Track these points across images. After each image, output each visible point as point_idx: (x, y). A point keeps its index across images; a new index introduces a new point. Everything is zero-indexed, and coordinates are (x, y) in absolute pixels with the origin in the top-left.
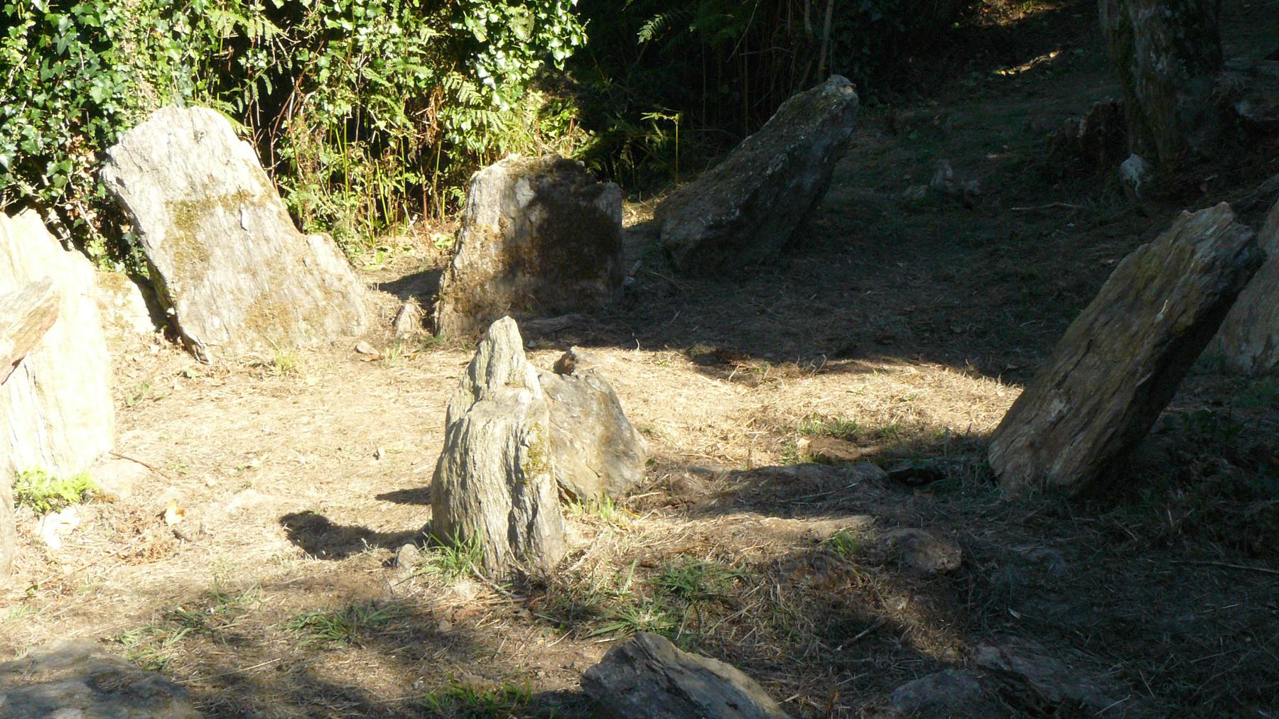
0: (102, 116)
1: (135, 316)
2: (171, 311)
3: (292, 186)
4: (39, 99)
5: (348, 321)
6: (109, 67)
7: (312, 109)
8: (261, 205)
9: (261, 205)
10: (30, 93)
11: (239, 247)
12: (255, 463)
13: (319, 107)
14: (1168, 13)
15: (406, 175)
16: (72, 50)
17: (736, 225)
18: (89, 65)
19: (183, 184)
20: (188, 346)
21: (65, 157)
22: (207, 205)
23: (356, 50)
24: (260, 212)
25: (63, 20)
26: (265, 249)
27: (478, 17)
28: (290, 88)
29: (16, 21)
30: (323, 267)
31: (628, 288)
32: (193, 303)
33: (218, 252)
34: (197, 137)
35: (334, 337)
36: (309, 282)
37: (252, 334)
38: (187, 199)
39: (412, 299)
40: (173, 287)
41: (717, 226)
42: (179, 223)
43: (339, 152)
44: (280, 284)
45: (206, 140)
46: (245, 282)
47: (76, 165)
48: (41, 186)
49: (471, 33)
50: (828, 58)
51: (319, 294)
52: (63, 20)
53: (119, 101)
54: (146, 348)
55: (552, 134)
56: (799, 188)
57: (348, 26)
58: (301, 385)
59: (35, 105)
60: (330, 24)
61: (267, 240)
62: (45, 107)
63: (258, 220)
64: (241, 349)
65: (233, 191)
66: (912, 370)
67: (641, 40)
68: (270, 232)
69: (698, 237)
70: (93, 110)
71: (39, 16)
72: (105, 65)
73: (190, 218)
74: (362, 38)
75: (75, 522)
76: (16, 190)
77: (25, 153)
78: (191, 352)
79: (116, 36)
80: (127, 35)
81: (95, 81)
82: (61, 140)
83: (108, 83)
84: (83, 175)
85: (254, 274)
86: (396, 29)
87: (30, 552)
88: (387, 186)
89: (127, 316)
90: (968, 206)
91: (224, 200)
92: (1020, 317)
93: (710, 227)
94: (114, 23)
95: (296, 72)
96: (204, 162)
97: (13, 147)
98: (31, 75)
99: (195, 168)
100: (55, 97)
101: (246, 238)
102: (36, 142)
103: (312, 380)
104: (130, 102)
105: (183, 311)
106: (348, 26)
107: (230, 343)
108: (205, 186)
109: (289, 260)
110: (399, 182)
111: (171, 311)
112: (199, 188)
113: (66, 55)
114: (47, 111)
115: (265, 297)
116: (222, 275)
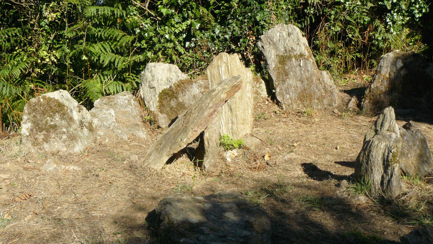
0: (259, 25)
1: (262, 91)
2: (274, 91)
3: (317, 54)
4: (240, 18)
5: (331, 101)
6: (263, 10)
7: (327, 28)
8: (307, 59)
9: (307, 59)
10: (237, 16)
11: (298, 72)
12: (295, 144)
13: (329, 28)
15: (357, 54)
16: (252, 3)
18: (257, 8)
19: (283, 50)
20: (278, 103)
21: (246, 38)
22: (290, 58)
23: (344, 9)
24: (307, 61)
26: (307, 74)
28: (321, 21)
30: (326, 82)
32: (281, 89)
33: (292, 73)
34: (289, 34)
35: (326, 106)
36: (320, 87)
37: (299, 102)
38: (283, 55)
39: (354, 97)
40: (276, 83)
42: (280, 63)
43: (334, 44)
44: (311, 86)
45: (292, 36)
46: (299, 84)
47: (249, 40)
48: (238, 46)
51: (323, 91)
53: (265, 21)
55: (411, 44)
58: (313, 121)
59: (239, 20)
61: (308, 71)
62: (242, 21)
63: (306, 64)
65: (299, 54)
68: (309, 68)
70: (256, 23)
72: (262, 9)
73: (284, 61)
75: (236, 154)
76: (230, 47)
77: (234, 35)
78: (278, 105)
81: (258, 14)
82: (245, 32)
83: (262, 15)
84: (251, 44)
85: (302, 82)
87: (222, 161)
88: (349, 57)
89: (259, 91)
91: (295, 56)
96: (290, 43)
97: (230, 33)
99: (287, 45)
100: (245, 18)
101: (301, 70)
104: (268, 21)
107: (292, 104)
108: (290, 51)
109: (314, 79)
110: (354, 56)
111: (274, 91)
112: (288, 51)
113: (250, 5)
114: (242, 22)
115: (305, 90)
116: (291, 81)
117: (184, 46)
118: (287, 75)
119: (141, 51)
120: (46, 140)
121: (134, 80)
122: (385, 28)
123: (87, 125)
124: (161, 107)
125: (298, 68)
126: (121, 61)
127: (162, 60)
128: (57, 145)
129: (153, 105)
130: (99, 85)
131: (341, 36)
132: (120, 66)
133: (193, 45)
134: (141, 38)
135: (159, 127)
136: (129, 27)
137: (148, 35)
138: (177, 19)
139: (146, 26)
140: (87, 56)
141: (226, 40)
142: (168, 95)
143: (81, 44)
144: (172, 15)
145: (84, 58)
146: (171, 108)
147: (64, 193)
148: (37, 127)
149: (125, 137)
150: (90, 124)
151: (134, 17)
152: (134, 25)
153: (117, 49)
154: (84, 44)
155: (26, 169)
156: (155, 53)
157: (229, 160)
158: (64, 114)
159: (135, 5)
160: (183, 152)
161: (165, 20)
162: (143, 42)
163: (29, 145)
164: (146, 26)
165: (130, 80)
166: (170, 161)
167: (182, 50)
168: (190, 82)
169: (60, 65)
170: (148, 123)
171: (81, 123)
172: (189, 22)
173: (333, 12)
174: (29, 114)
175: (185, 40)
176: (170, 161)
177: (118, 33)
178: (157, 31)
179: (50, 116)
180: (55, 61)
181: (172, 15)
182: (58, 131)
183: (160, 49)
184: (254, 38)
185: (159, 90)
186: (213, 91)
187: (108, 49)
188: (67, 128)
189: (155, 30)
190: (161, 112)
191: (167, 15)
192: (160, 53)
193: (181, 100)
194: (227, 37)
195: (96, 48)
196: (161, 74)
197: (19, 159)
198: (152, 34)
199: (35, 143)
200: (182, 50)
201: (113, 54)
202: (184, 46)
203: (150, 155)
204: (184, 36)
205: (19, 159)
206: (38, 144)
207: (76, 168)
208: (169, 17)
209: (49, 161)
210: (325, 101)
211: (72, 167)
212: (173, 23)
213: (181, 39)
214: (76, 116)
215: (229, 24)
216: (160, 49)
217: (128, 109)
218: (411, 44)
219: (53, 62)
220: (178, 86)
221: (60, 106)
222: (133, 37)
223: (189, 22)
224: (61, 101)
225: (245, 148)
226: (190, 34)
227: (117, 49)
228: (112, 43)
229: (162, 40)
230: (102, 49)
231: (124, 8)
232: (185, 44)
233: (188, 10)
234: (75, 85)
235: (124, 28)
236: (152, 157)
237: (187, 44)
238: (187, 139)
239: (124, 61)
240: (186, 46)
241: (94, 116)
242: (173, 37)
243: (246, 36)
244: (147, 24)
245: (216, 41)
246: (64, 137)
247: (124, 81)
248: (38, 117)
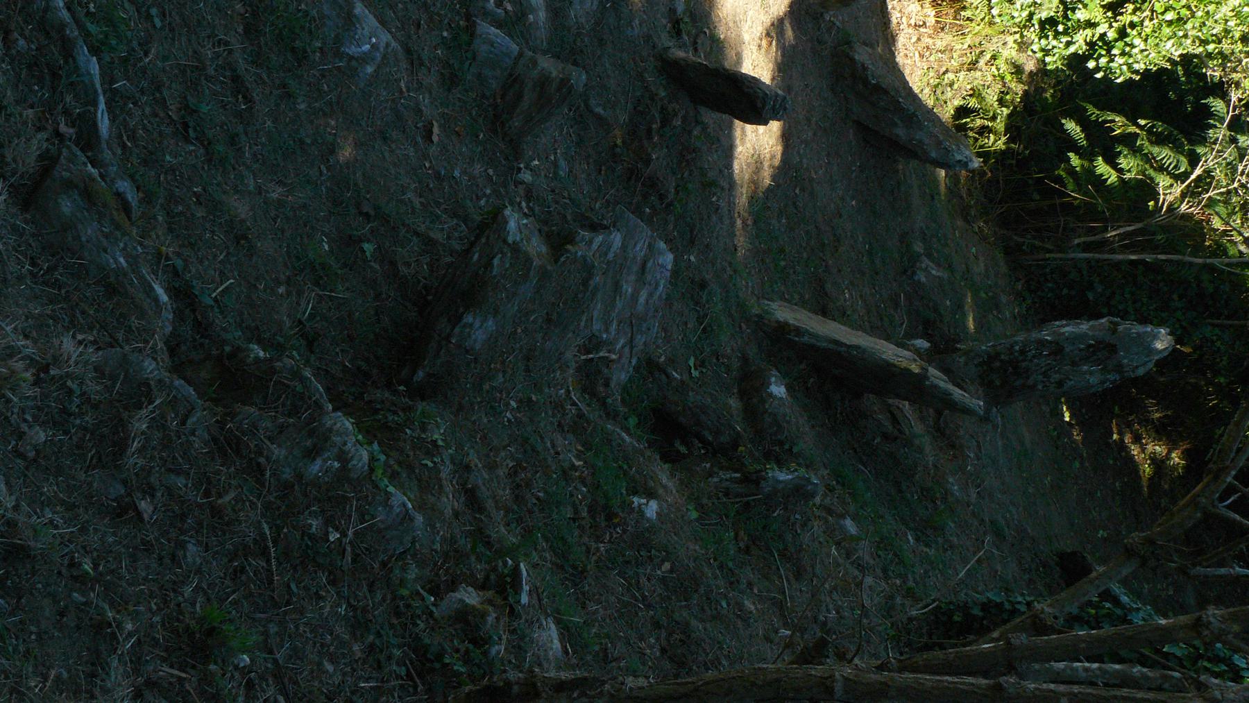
14: (1017, 348)
17: (866, 82)
31: (822, 14)
41: (864, 68)
50: (1055, 259)
56: (896, 125)
67: (1063, 121)
69: (857, 57)
90: (906, 271)
92: (807, 232)
93: (863, 65)
218: (994, 68)
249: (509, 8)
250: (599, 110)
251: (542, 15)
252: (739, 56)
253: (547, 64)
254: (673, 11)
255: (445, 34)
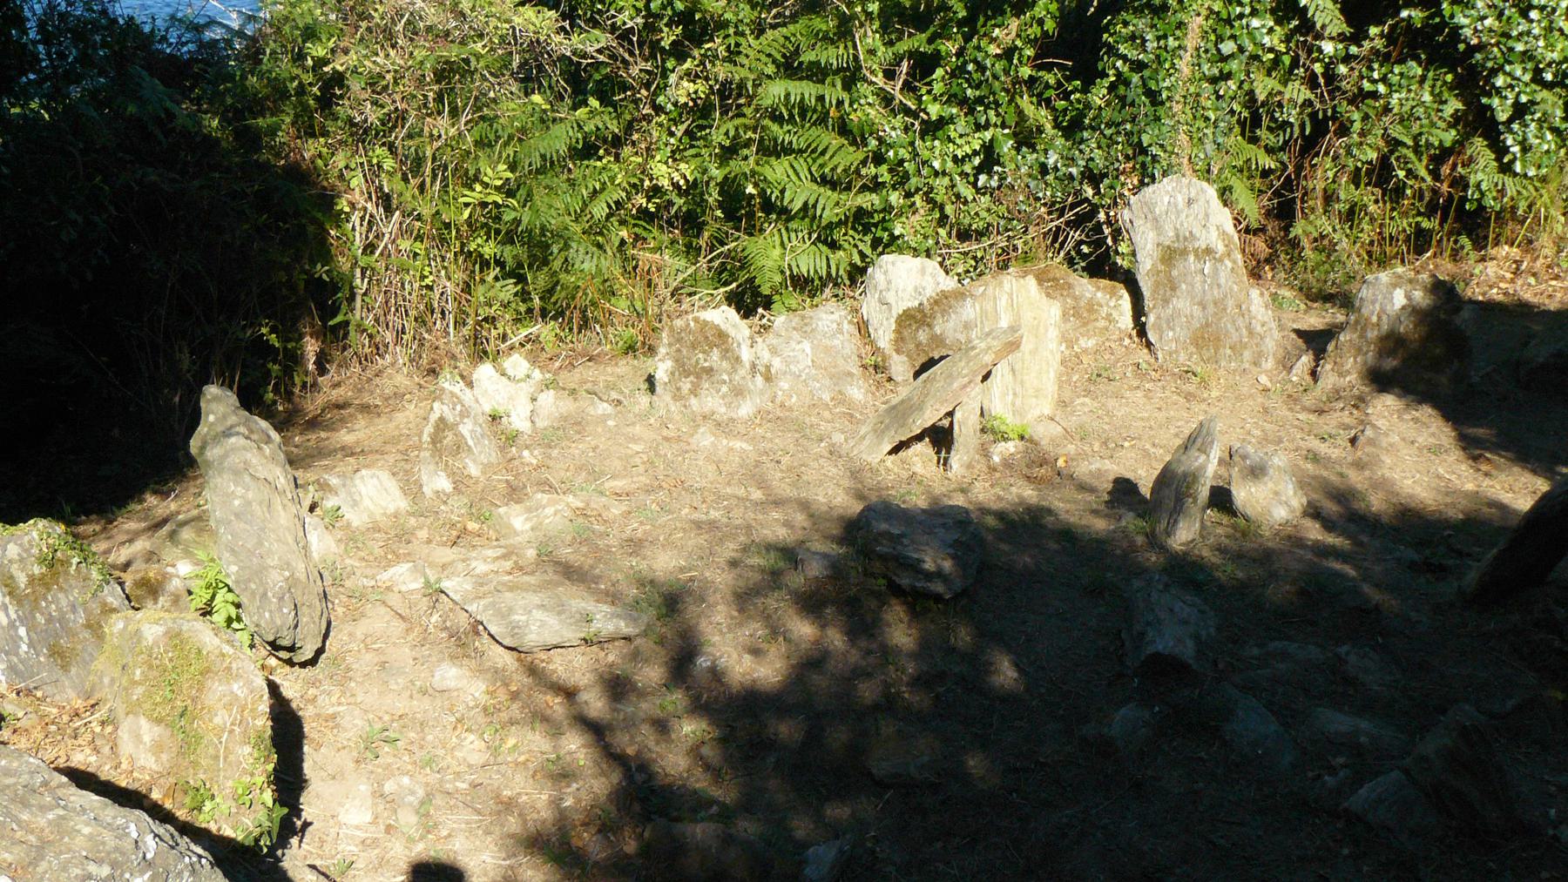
1: (1121, 314)
4: (1108, 132)
8: (1221, 260)
9: (1221, 260)
12: (1126, 444)
13: (1349, 153)
19: (1171, 234)
20: (1149, 345)
22: (1184, 253)
23: (1387, 110)
25: (1136, 79)
27: (1506, 98)
29: (1104, 75)
32: (1159, 318)
34: (1190, 202)
36: (1240, 322)
37: (1192, 349)
40: (1148, 303)
45: (1195, 206)
47: (1123, 185)
49: (1493, 110)
52: (1136, 79)
53: (1162, 146)
54: (1121, 339)
57: (1382, 88)
60: (1367, 86)
61: (1219, 286)
63: (1216, 271)
64: (1182, 357)
66: (1486, 510)
68: (1222, 281)
69: (1541, 360)
71: (1119, 74)
72: (1157, 119)
73: (1170, 258)
74: (1394, 101)
75: (1012, 450)
76: (1077, 193)
79: (1169, 98)
80: (1177, 98)
85: (1204, 308)
86: (1427, 98)
91: (1196, 251)
94: (1168, 88)
95: (1334, 118)
96: (1189, 223)
98: (1107, 114)
102: (1100, 162)
103: (1215, 393)
105: (1151, 320)
106: (1382, 88)
108: (1185, 239)
109: (1230, 303)
113: (1132, 104)
114: (1112, 142)
115: (1207, 325)
116: (1181, 303)
117: (975, 185)
118: (1173, 289)
119: (875, 186)
120: (694, 392)
121: (856, 246)
122: (1499, 159)
123: (763, 369)
124: (899, 340)
125: (1199, 278)
126: (830, 204)
127: (922, 212)
128: (711, 401)
129: (884, 337)
130: (778, 251)
131: (1380, 173)
132: (829, 216)
133: (994, 183)
134: (879, 159)
135: (890, 379)
136: (855, 130)
137: (896, 154)
138: (962, 125)
139: (893, 134)
140: (756, 185)
141: (1071, 177)
142: (913, 319)
143: (746, 158)
144: (951, 120)
145: (750, 189)
146: (918, 345)
147: (729, 484)
148: (682, 369)
149: (826, 397)
150: (768, 368)
151: (868, 111)
152: (866, 128)
153: (823, 177)
154: (752, 160)
155: (666, 439)
156: (908, 195)
157: (996, 459)
158: (727, 351)
159: (872, 83)
160: (919, 438)
161: (933, 128)
162: (884, 167)
163: (668, 398)
164: (893, 134)
165: (846, 245)
166: (895, 450)
167: (967, 192)
168: (960, 295)
169: (692, 190)
170: (871, 370)
171: (754, 366)
172: (988, 135)
173: (1356, 116)
174: (670, 345)
175: (979, 170)
176: (895, 450)
177: (833, 140)
178: (914, 149)
179: (704, 352)
180: (682, 182)
181: (951, 120)
182: (714, 379)
183: (918, 190)
184: (1136, 182)
185: (898, 309)
186: (973, 348)
187: (804, 173)
188: (730, 374)
189: (912, 144)
190: (898, 351)
191: (941, 118)
192: (917, 199)
193: (938, 330)
194: (1074, 171)
195: (777, 170)
196: (903, 279)
197: (652, 421)
198: (904, 153)
199: (678, 396)
200: (967, 192)
201: (815, 187)
202: (975, 185)
203: (864, 438)
204: (977, 161)
205: (652, 421)
206: (682, 398)
207: (744, 445)
208: (942, 123)
209: (702, 430)
210: (1247, 354)
211: (738, 444)
212: (953, 135)
213: (968, 168)
214: (746, 354)
215: (1082, 141)
216: (918, 190)
217: (836, 342)
219: (676, 186)
220: (936, 302)
221: (722, 335)
222: (860, 156)
223: (988, 135)
224: (723, 327)
225: (1031, 441)
226: (990, 157)
227: (823, 177)
228: (814, 161)
229: (925, 172)
230: (791, 172)
231: (847, 87)
232: (977, 180)
233: (987, 107)
234: (722, 244)
235: (843, 129)
236: (866, 442)
237: (983, 178)
238: (930, 416)
239: (837, 204)
240: (980, 184)
241: (774, 351)
242: (950, 164)
243: (1119, 173)
244: (894, 128)
245: (1050, 178)
246: (724, 389)
247: (834, 246)
248: (685, 352)
249: (1341, 760)
250: (1510, 704)
251: (1364, 724)
252: (1502, 507)
253: (1430, 745)
254: (1412, 565)
255: (1346, 851)
